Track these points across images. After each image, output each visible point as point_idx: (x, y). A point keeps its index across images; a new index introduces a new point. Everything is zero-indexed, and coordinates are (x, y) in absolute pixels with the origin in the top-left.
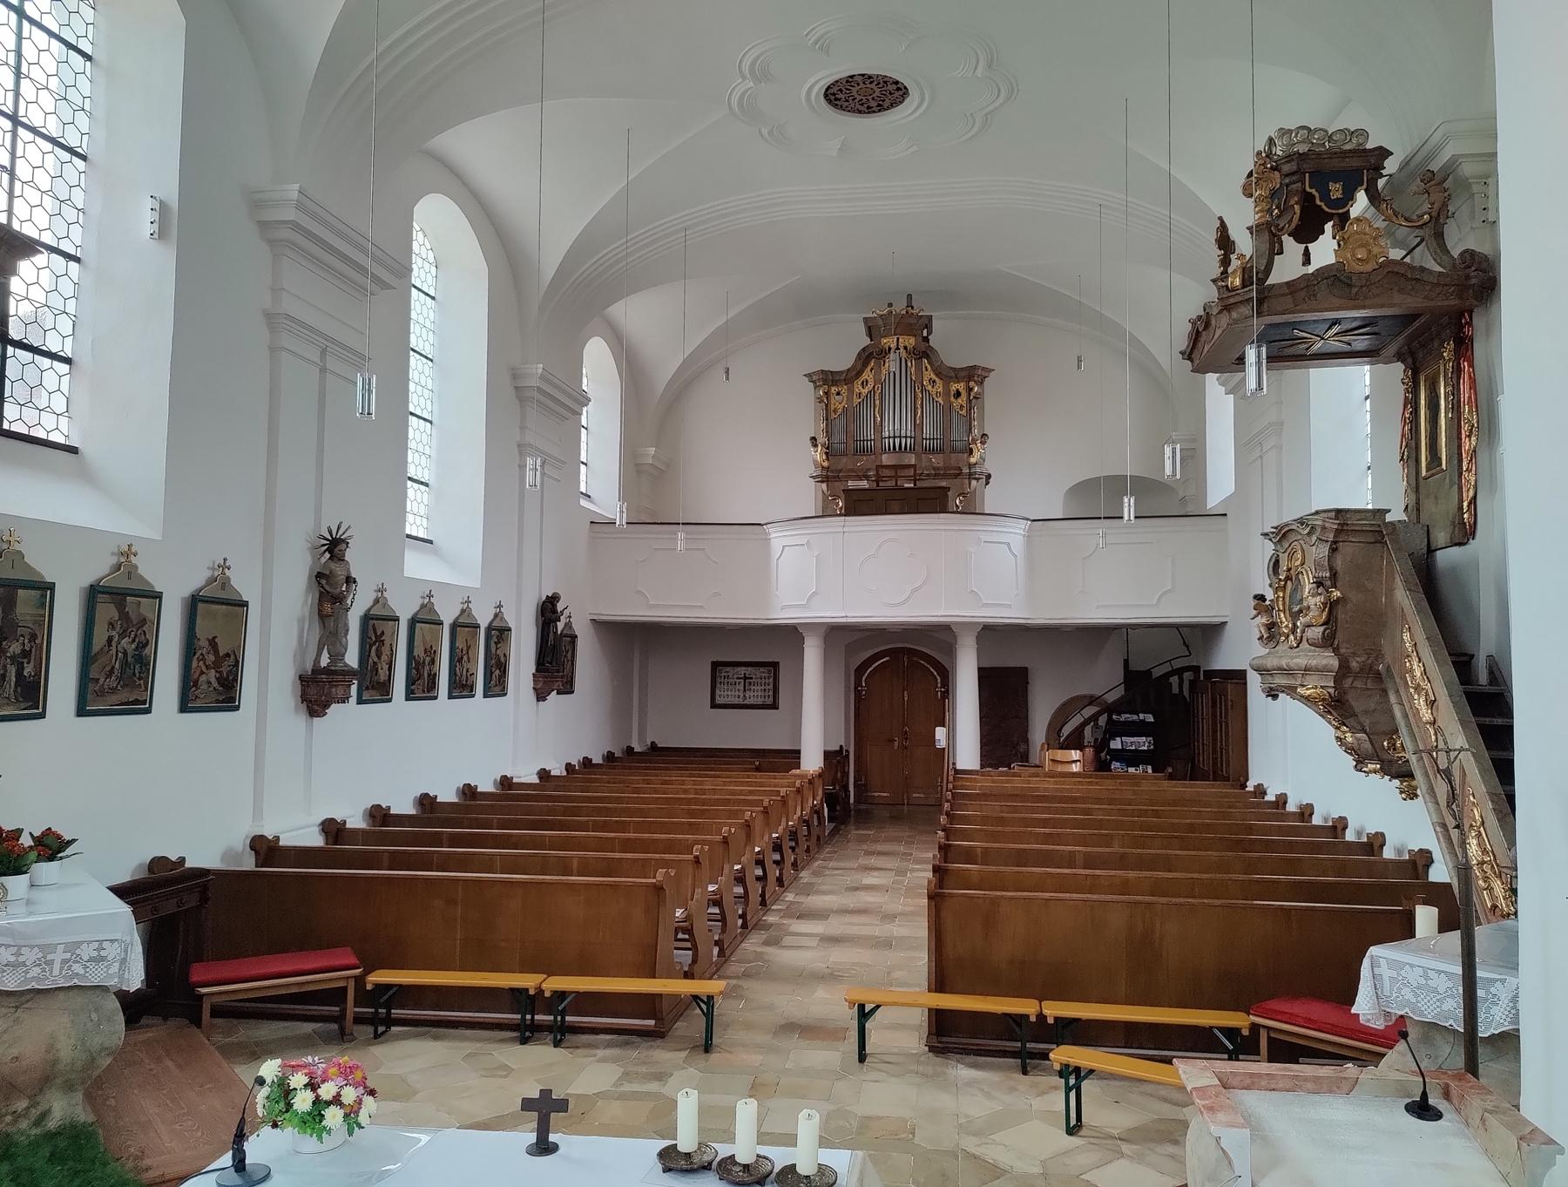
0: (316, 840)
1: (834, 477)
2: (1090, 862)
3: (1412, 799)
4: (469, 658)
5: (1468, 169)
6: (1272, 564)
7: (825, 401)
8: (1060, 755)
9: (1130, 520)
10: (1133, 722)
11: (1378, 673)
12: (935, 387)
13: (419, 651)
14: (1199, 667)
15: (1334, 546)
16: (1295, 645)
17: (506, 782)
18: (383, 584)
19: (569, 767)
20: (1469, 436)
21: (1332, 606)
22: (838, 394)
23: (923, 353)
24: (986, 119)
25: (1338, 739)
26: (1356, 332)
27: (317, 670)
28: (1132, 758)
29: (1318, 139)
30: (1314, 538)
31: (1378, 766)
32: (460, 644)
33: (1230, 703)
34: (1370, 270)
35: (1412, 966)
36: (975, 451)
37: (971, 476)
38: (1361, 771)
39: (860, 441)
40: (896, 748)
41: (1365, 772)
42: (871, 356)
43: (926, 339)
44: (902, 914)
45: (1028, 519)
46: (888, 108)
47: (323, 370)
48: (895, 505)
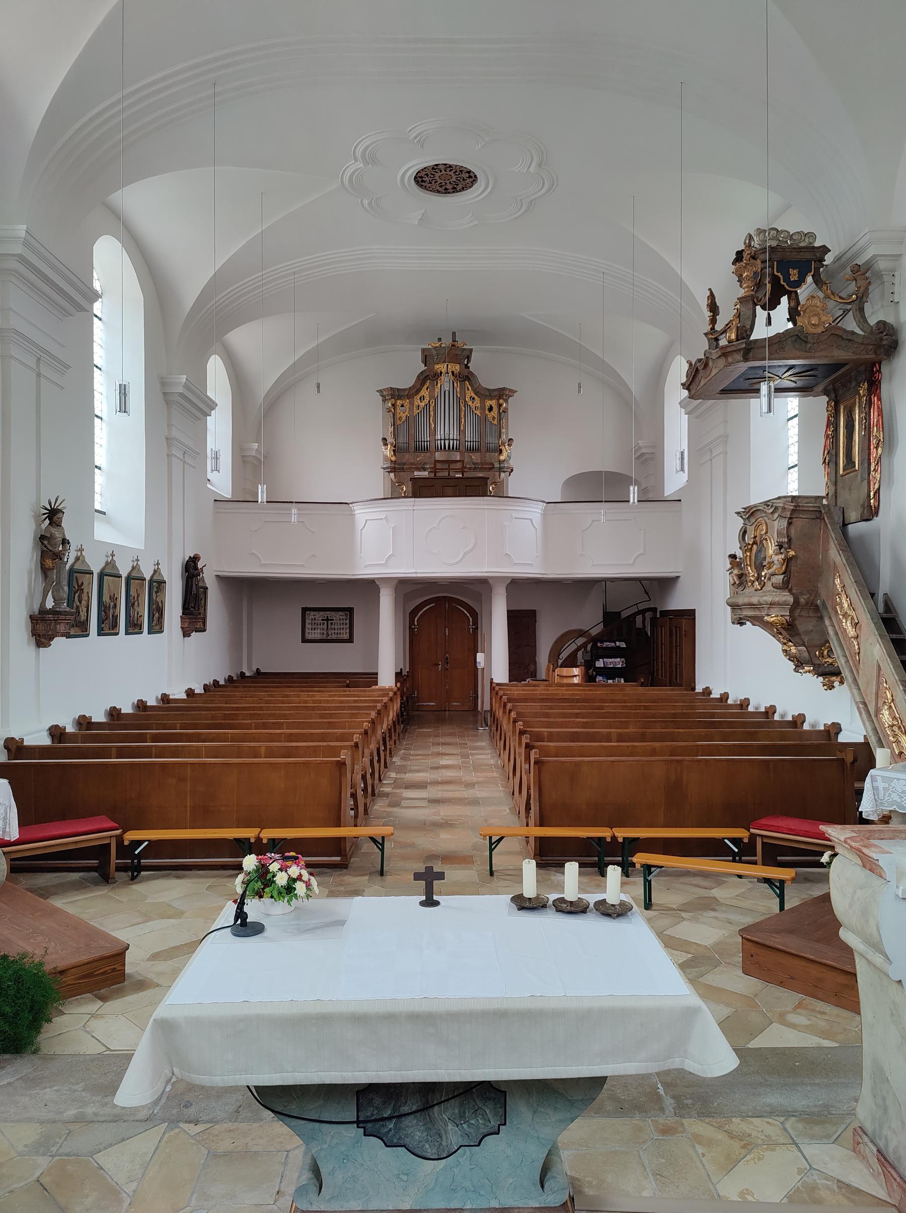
0: (46, 741)
1: (400, 469)
2: (621, 738)
3: (831, 689)
4: (138, 604)
5: (882, 265)
6: (741, 533)
7: (393, 411)
8: (565, 671)
9: (634, 502)
10: (612, 648)
11: (817, 606)
12: (474, 403)
13: (106, 598)
14: (656, 609)
15: (790, 521)
16: (760, 588)
17: (165, 698)
18: (81, 545)
19: (206, 687)
20: (877, 448)
21: (788, 561)
22: (402, 406)
23: (465, 377)
24: (531, 204)
25: (785, 651)
26: (803, 374)
27: (43, 611)
28: (609, 673)
29: (783, 237)
30: (776, 515)
31: (812, 668)
32: (133, 593)
33: (684, 633)
34: (820, 331)
35: (898, 779)
36: (504, 451)
37: (501, 470)
38: (798, 672)
39: (473, 441)
40: (440, 670)
41: (801, 673)
42: (428, 378)
43: (467, 367)
44: (478, 783)
45: (544, 502)
46: (460, 191)
47: (39, 375)
48: (449, 490)
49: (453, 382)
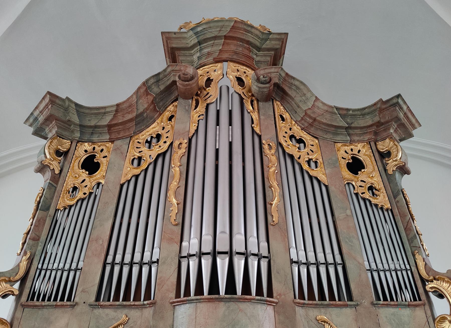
49: (241, 99)
